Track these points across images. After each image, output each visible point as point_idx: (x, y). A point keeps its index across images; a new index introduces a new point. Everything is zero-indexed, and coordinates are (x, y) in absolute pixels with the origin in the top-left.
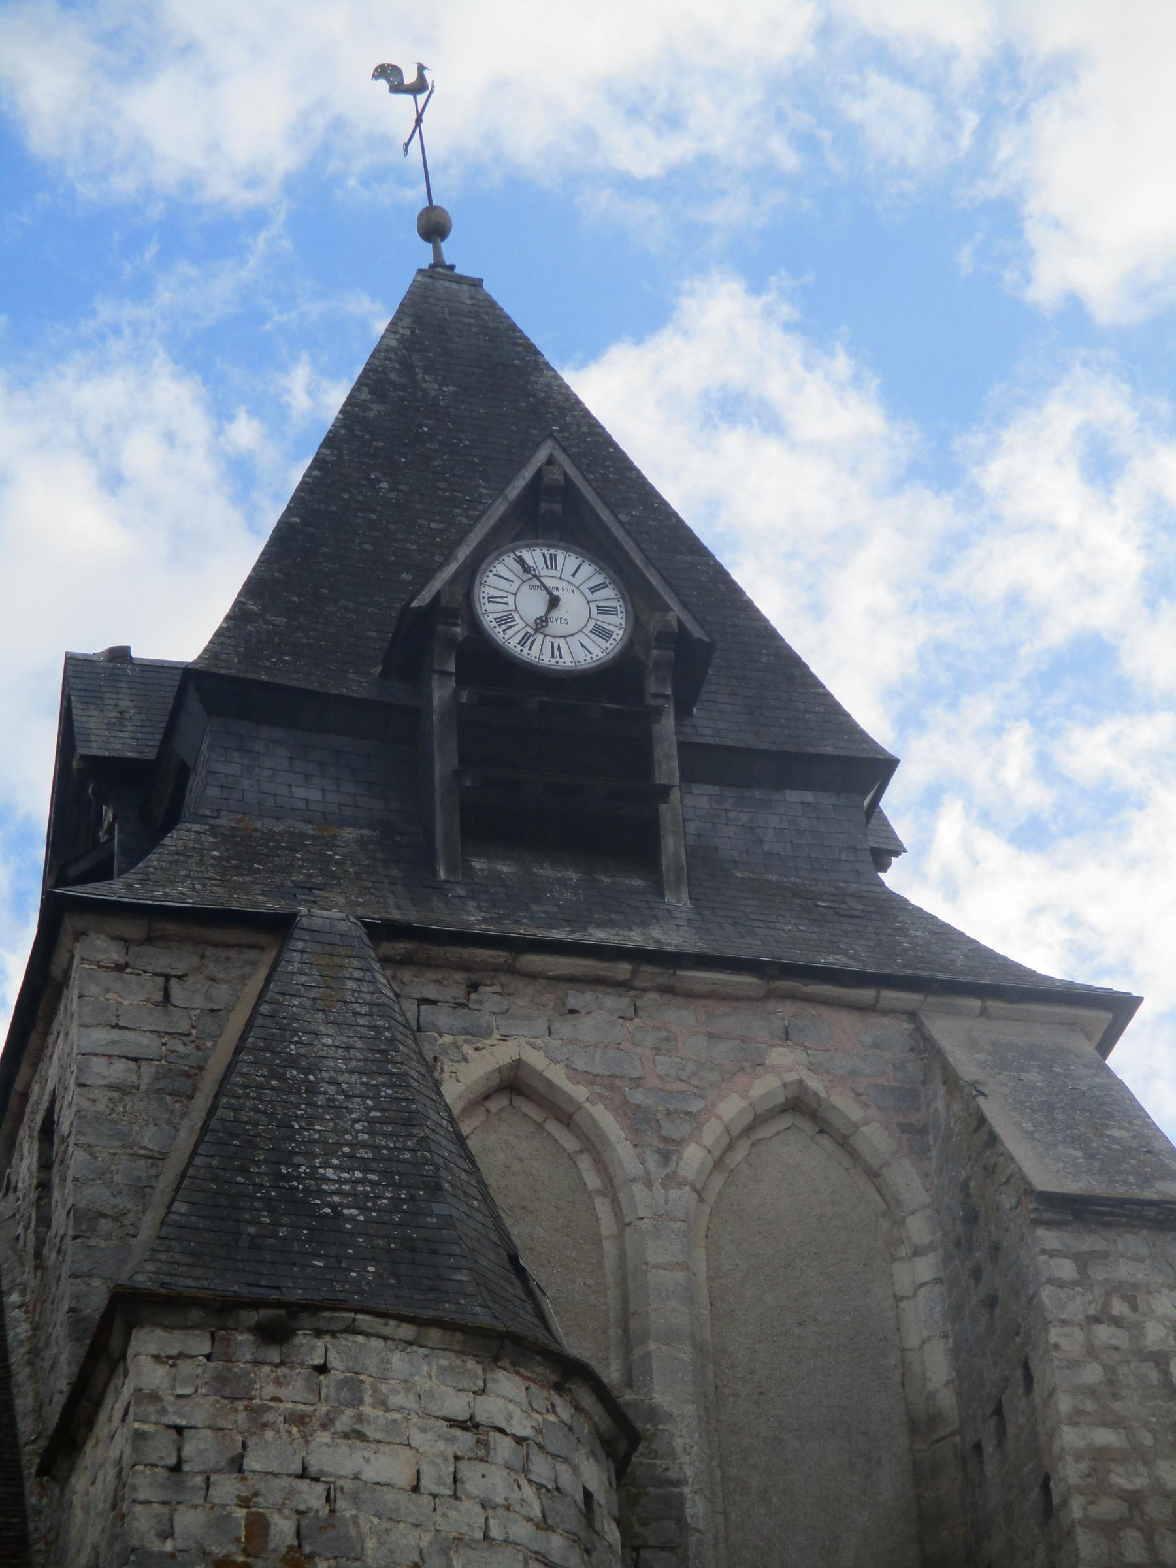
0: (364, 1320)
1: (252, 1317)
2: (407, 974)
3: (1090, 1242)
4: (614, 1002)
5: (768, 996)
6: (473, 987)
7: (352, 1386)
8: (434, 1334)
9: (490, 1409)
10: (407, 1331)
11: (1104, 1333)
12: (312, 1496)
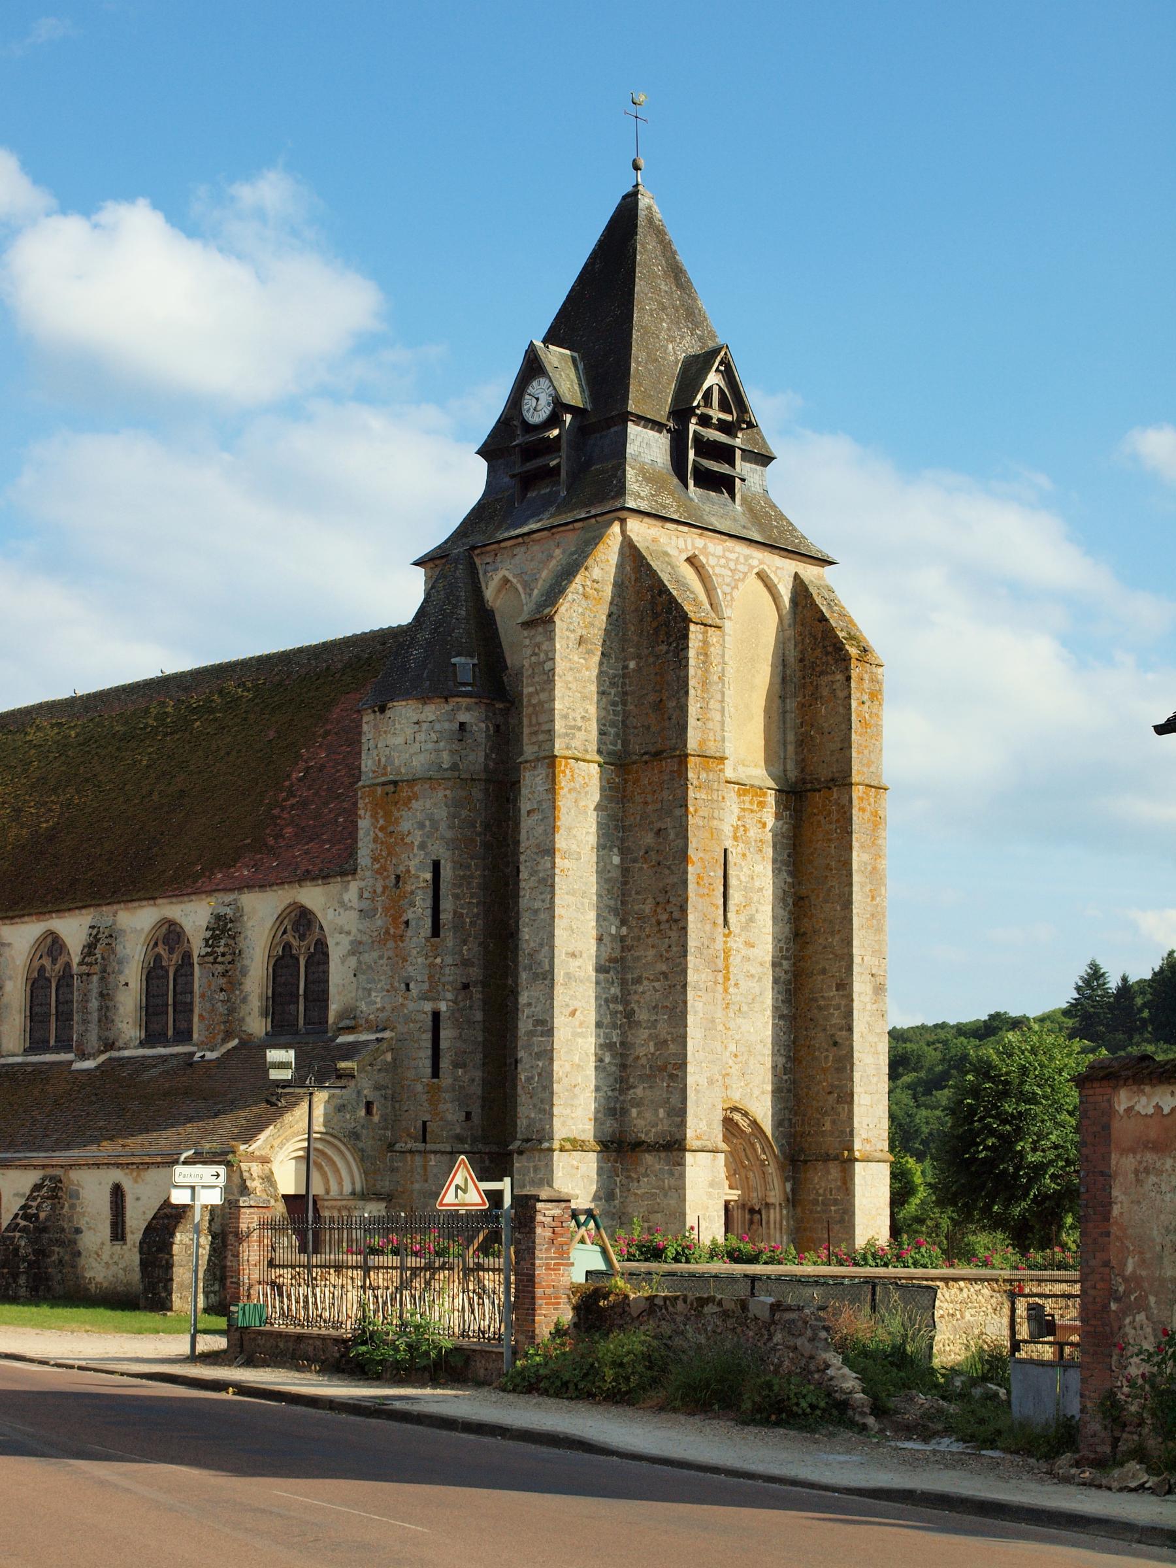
2: (483, 557)
4: (523, 549)
5: (553, 534)
9: (422, 717)
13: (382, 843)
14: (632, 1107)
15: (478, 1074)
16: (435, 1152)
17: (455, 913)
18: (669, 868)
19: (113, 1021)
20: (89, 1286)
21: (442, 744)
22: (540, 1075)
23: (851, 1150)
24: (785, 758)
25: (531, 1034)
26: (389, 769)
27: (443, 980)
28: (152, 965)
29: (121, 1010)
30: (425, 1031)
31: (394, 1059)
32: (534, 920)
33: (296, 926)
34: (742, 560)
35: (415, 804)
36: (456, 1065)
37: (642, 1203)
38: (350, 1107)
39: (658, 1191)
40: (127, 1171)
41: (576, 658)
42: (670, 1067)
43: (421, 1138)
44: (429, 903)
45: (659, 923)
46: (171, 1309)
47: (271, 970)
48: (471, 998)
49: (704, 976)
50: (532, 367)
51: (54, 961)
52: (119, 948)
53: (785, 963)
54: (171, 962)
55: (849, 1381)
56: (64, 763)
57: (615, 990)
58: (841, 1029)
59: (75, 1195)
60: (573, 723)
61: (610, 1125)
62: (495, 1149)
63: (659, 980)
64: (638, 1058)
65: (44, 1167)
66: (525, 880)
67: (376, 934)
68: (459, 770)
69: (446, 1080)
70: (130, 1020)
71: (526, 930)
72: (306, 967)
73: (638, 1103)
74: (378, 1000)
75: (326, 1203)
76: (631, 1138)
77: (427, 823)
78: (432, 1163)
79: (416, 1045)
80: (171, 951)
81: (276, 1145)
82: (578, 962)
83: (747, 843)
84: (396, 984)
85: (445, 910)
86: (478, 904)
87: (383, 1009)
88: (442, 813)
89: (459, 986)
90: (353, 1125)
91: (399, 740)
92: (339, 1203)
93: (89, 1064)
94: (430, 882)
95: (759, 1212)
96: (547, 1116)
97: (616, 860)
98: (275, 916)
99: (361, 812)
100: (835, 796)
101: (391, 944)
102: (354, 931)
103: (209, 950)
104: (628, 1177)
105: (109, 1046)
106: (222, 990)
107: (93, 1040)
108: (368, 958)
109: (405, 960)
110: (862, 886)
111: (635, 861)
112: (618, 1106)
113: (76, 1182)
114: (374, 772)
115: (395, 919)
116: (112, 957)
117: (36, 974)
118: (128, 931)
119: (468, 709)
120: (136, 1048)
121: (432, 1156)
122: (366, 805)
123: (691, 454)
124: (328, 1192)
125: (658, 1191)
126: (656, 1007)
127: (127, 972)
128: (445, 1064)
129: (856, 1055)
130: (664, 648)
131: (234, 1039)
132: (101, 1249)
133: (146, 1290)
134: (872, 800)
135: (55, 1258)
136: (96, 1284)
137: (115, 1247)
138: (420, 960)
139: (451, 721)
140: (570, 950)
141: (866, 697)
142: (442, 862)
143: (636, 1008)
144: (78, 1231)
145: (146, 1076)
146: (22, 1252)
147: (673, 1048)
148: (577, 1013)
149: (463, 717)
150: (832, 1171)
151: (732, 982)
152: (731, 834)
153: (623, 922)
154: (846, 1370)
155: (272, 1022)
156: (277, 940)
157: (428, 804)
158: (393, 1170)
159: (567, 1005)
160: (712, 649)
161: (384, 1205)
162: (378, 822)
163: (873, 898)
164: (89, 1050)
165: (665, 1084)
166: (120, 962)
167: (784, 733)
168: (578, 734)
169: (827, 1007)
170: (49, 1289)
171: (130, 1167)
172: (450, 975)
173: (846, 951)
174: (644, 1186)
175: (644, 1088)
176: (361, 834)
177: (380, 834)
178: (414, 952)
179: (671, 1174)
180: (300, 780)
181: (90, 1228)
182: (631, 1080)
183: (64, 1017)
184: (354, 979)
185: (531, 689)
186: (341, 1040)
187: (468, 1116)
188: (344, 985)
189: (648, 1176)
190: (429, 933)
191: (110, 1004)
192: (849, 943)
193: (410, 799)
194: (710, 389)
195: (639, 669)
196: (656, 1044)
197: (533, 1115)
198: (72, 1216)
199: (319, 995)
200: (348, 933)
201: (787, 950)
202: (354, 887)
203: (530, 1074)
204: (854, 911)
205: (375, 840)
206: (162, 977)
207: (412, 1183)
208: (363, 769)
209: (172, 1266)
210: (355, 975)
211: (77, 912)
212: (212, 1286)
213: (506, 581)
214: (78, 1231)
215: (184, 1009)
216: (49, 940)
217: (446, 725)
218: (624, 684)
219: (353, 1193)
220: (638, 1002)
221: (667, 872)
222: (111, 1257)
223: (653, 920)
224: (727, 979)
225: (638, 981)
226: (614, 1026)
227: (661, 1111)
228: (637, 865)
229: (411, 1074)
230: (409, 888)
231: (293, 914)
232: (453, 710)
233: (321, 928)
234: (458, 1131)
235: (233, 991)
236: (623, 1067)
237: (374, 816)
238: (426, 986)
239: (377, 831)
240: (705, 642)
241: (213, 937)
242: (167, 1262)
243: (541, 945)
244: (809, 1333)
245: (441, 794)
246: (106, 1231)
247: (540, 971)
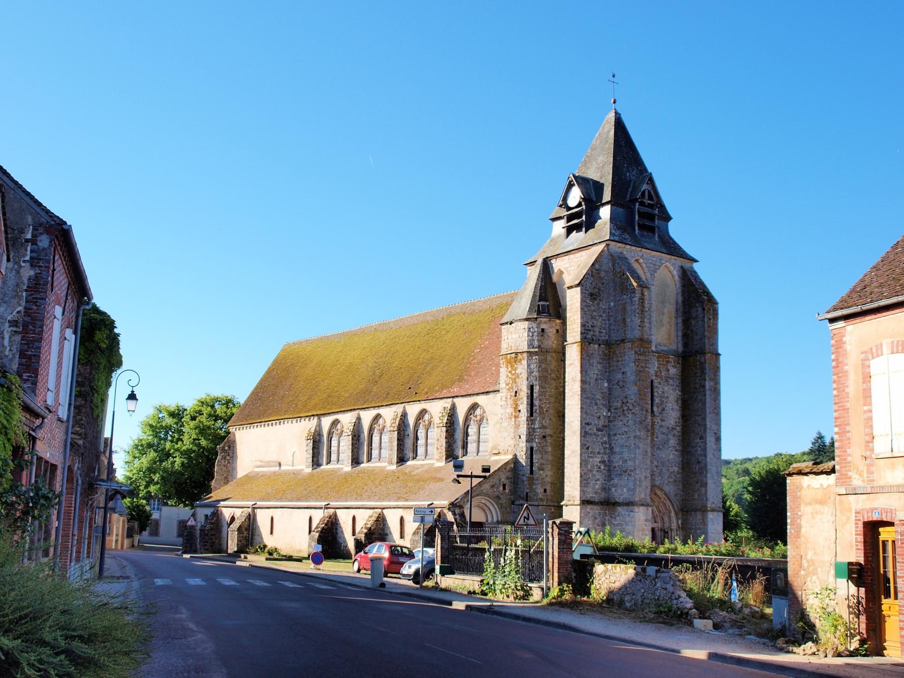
11: (571, 302)
17: (540, 406)
18: (628, 388)
24: (677, 343)
31: (514, 467)
34: (658, 260)
41: (589, 302)
42: (628, 471)
45: (623, 410)
49: (642, 433)
53: (678, 428)
55: (689, 604)
56: (386, 346)
58: (702, 456)
62: (556, 504)
64: (615, 467)
65: (373, 508)
76: (613, 501)
82: (590, 427)
83: (661, 378)
92: (492, 526)
95: (667, 532)
97: (606, 385)
100: (698, 358)
103: (441, 421)
104: (612, 517)
110: (710, 395)
111: (613, 385)
112: (607, 487)
119: (545, 323)
123: (637, 217)
126: (622, 446)
129: (709, 467)
130: (625, 297)
134: (714, 360)
140: (587, 422)
141: (711, 317)
145: (415, 472)
147: (630, 463)
148: (590, 448)
149: (543, 326)
150: (698, 516)
151: (655, 436)
152: (654, 374)
153: (609, 410)
154: (688, 599)
159: (585, 445)
160: (645, 297)
163: (715, 401)
167: (677, 332)
168: (590, 333)
169: (695, 447)
177: (509, 375)
179: (629, 515)
180: (478, 352)
182: (612, 476)
187: (545, 491)
192: (704, 419)
194: (644, 191)
195: (615, 306)
201: (679, 422)
204: (707, 406)
218: (609, 312)
224: (653, 434)
225: (615, 435)
226: (605, 453)
227: (625, 489)
228: (615, 387)
229: (521, 473)
236: (609, 471)
237: (507, 367)
240: (643, 294)
241: (442, 416)
244: (672, 583)
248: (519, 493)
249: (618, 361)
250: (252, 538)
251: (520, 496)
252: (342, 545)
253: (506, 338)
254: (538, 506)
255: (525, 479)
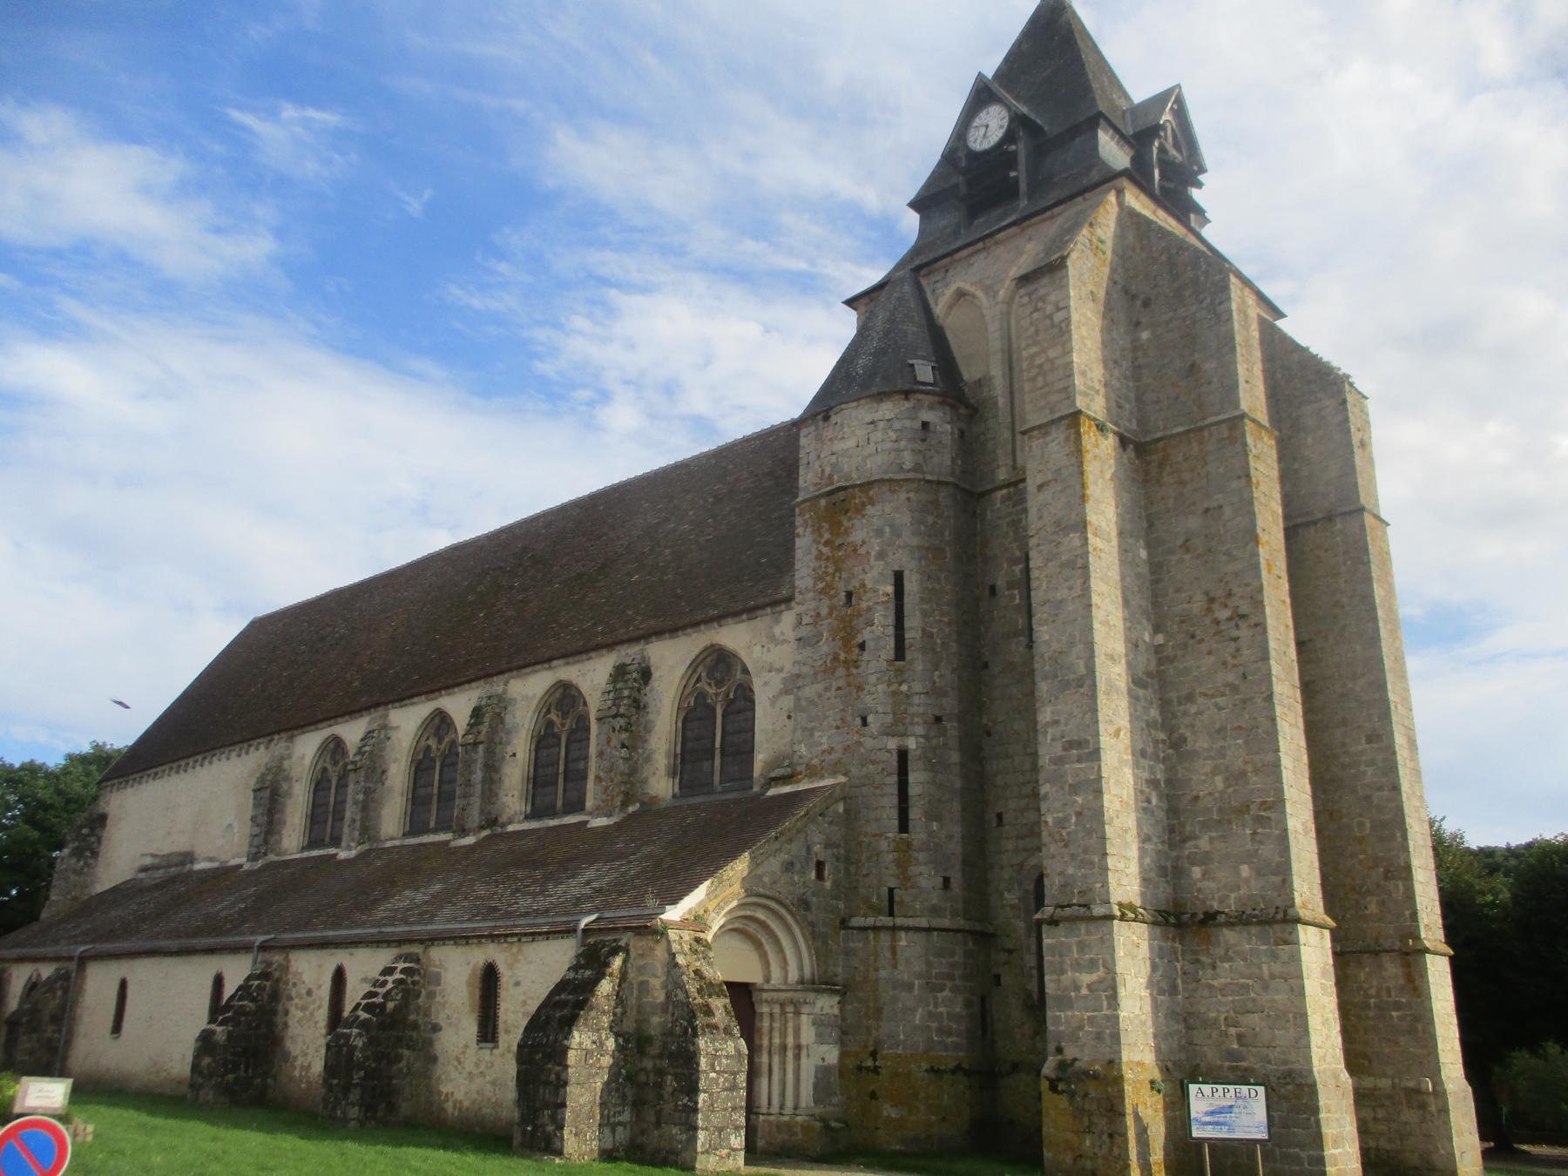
0: (843, 406)
1: (820, 417)
3: (1031, 288)
4: (982, 256)
6: (947, 271)
7: (842, 425)
8: (862, 401)
9: (879, 415)
10: (855, 404)
11: (1035, 315)
12: (833, 459)
13: (828, 559)
14: (1193, 864)
15: (957, 830)
16: (908, 929)
17: (924, 630)
18: (1228, 553)
19: (497, 795)
20: (446, 1105)
21: (903, 444)
22: (1079, 814)
23: (1417, 938)
25: (1058, 761)
26: (835, 477)
27: (912, 710)
28: (542, 732)
29: (507, 783)
30: (889, 774)
32: (1057, 615)
33: (711, 672)
35: (870, 510)
36: (931, 816)
37: (1224, 999)
38: (798, 867)
39: (1250, 982)
40: (505, 945)
43: (887, 909)
44: (891, 620)
45: (1217, 622)
46: (560, 1153)
47: (680, 724)
48: (944, 735)
50: (982, 95)
51: (440, 740)
52: (508, 719)
54: (563, 726)
57: (1154, 713)
58: (1380, 789)
59: (437, 979)
60: (1091, 384)
61: (1164, 891)
62: (978, 927)
63: (1223, 695)
64: (1197, 798)
66: (1039, 568)
67: (820, 662)
68: (923, 473)
69: (918, 835)
70: (516, 793)
71: (1045, 628)
72: (723, 716)
73: (1204, 860)
74: (824, 740)
75: (765, 996)
77: (887, 529)
78: (903, 943)
79: (878, 791)
80: (565, 715)
81: (711, 909)
84: (849, 718)
85: (911, 628)
86: (949, 623)
87: (831, 751)
88: (905, 518)
89: (931, 719)
90: (802, 890)
91: (851, 443)
92: (782, 996)
93: (470, 840)
94: (892, 596)
96: (1096, 870)
97: (1143, 554)
98: (688, 662)
99: (800, 530)
101: (841, 671)
102: (788, 666)
105: (492, 822)
106: (623, 746)
107: (474, 817)
108: (810, 691)
109: (860, 688)
113: (437, 963)
114: (815, 485)
115: (846, 642)
116: (500, 726)
117: (421, 756)
118: (519, 699)
119: (931, 407)
120: (520, 822)
121: (903, 934)
122: (806, 521)
124: (767, 979)
125: (1250, 982)
126: (1222, 729)
127: (515, 742)
128: (915, 814)
131: (634, 804)
132: (464, 1053)
133: (524, 1120)
135: (403, 1064)
136: (455, 1102)
137: (483, 1051)
138: (881, 688)
139: (913, 419)
142: (906, 573)
143: (1188, 734)
144: (436, 1028)
146: (358, 1054)
147: (1255, 781)
149: (926, 416)
153: (1157, 629)
155: (680, 782)
156: (689, 689)
157: (888, 508)
158: (848, 952)
161: (837, 999)
162: (821, 536)
164: (469, 825)
165: (1248, 832)
166: (509, 733)
170: (392, 1107)
171: (509, 940)
172: (920, 706)
173: (1377, 696)
174: (1225, 974)
175: (1211, 839)
176: (799, 554)
177: (825, 550)
178: (873, 679)
179: (1274, 956)
181: (450, 1025)
182: (1188, 828)
183: (446, 798)
184: (787, 721)
185: (1034, 350)
186: (772, 792)
187: (946, 881)
188: (774, 731)
189: (1230, 959)
190: (891, 655)
191: (496, 777)
193: (864, 505)
196: (1226, 779)
197: (1071, 871)
198: (430, 1007)
199: (740, 749)
200: (780, 670)
202: (788, 618)
203: (1060, 815)
205: (818, 558)
206: (554, 746)
207: (877, 970)
208: (801, 483)
209: (565, 1084)
210: (789, 717)
211: (467, 686)
212: (620, 1113)
213: (961, 294)
214: (436, 1028)
215: (577, 777)
216: (437, 721)
217: (908, 423)
219: (802, 981)
220: (1193, 726)
221: (1224, 558)
222: (477, 1065)
223: (1208, 621)
225: (1190, 698)
227: (1245, 871)
228: (1174, 558)
229: (871, 828)
230: (864, 605)
231: (709, 660)
232: (914, 408)
233: (746, 671)
234: (935, 901)
235: (635, 748)
237: (818, 531)
238: (889, 719)
239: (821, 547)
242: (558, 1077)
243: (1072, 644)
245: (903, 496)
246: (470, 1027)
247: (1071, 676)
248: (863, 891)
249: (1182, 483)
250: (68, 1043)
251: (867, 900)
252: (298, 1063)
253: (813, 456)
254: (929, 930)
255: (884, 845)
